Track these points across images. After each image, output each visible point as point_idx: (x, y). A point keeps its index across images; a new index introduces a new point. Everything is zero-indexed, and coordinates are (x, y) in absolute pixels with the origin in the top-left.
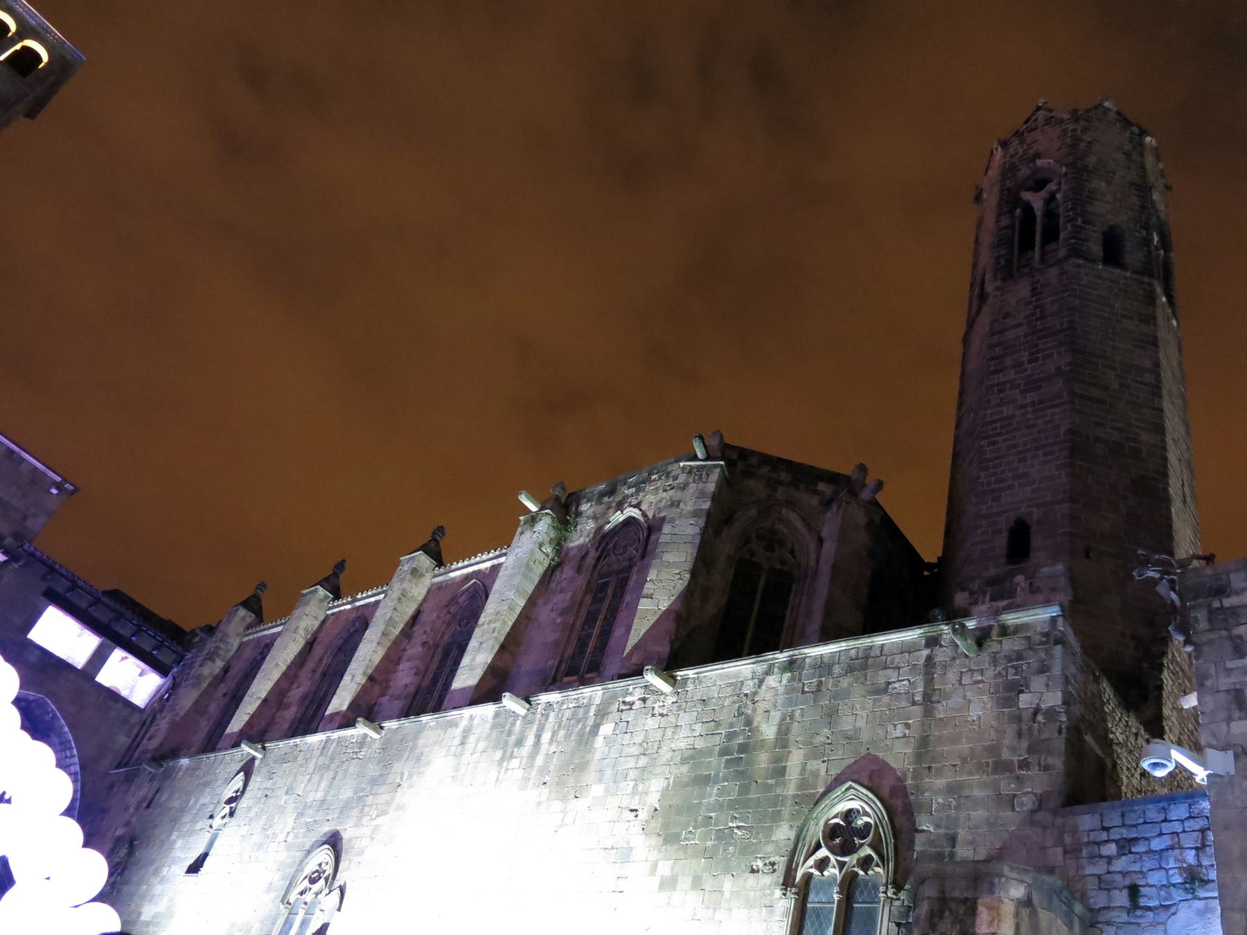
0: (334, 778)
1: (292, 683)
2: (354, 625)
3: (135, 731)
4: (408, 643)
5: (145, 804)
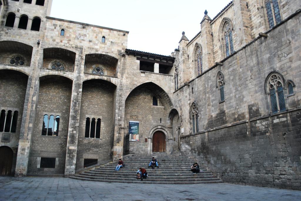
0: (257, 55)
1: (213, 46)
3: (174, 81)
4: (250, 12)
5: (191, 93)
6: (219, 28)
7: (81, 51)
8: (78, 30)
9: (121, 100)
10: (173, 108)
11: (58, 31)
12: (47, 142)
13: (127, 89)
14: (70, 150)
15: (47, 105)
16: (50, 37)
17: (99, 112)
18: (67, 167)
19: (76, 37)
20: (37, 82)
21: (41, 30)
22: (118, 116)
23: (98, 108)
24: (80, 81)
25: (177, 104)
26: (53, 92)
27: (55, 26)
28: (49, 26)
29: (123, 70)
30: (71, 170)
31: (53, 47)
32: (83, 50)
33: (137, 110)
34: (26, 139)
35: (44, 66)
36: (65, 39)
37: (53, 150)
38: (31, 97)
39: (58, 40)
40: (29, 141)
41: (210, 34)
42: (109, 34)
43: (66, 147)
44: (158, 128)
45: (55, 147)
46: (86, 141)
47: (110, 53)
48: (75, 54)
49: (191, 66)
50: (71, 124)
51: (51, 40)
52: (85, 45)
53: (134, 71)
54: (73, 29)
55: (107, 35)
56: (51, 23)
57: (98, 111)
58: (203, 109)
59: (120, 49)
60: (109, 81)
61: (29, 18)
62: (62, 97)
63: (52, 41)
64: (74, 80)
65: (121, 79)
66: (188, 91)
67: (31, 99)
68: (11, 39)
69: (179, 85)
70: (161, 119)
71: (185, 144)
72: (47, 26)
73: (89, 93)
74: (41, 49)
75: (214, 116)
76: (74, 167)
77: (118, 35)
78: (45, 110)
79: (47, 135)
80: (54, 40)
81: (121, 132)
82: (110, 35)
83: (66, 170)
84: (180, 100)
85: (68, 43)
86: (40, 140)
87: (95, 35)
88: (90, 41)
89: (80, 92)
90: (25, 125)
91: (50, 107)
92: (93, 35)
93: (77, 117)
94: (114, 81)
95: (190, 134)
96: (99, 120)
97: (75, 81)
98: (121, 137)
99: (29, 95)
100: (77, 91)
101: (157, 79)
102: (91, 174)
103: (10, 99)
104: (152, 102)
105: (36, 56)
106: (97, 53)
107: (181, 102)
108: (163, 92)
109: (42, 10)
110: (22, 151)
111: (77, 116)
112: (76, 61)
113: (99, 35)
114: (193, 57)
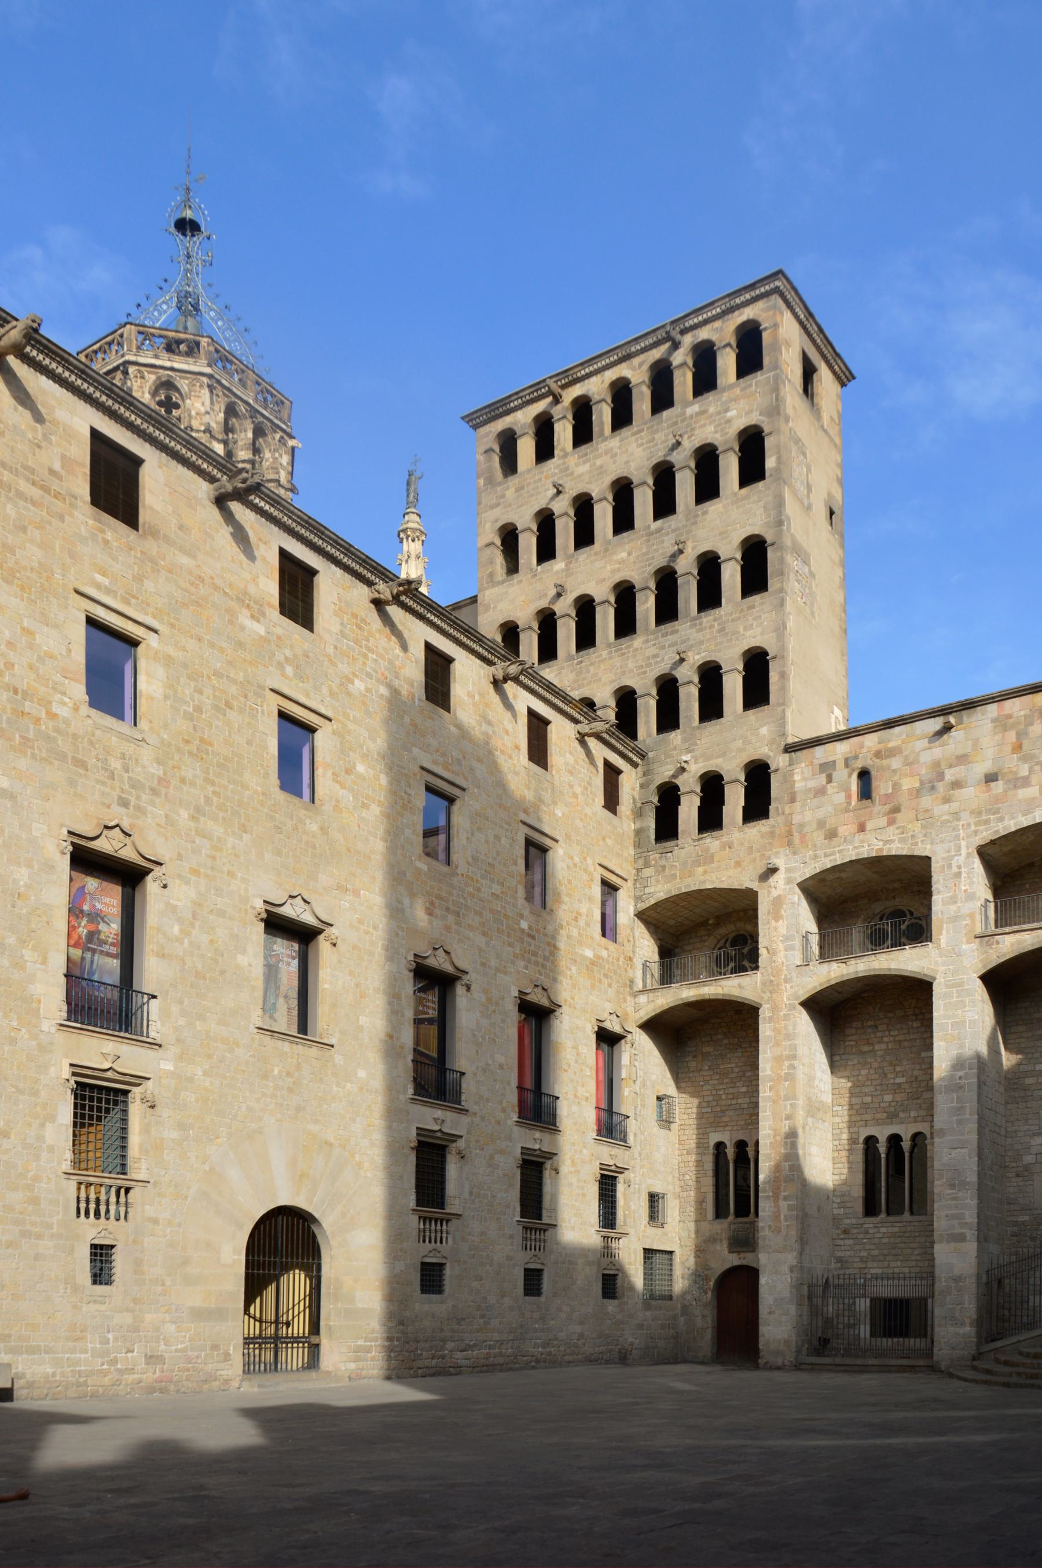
19: (922, 783)
27: (827, 768)
28: (804, 779)
54: (905, 753)
56: (812, 763)
72: (797, 785)
109: (765, 725)
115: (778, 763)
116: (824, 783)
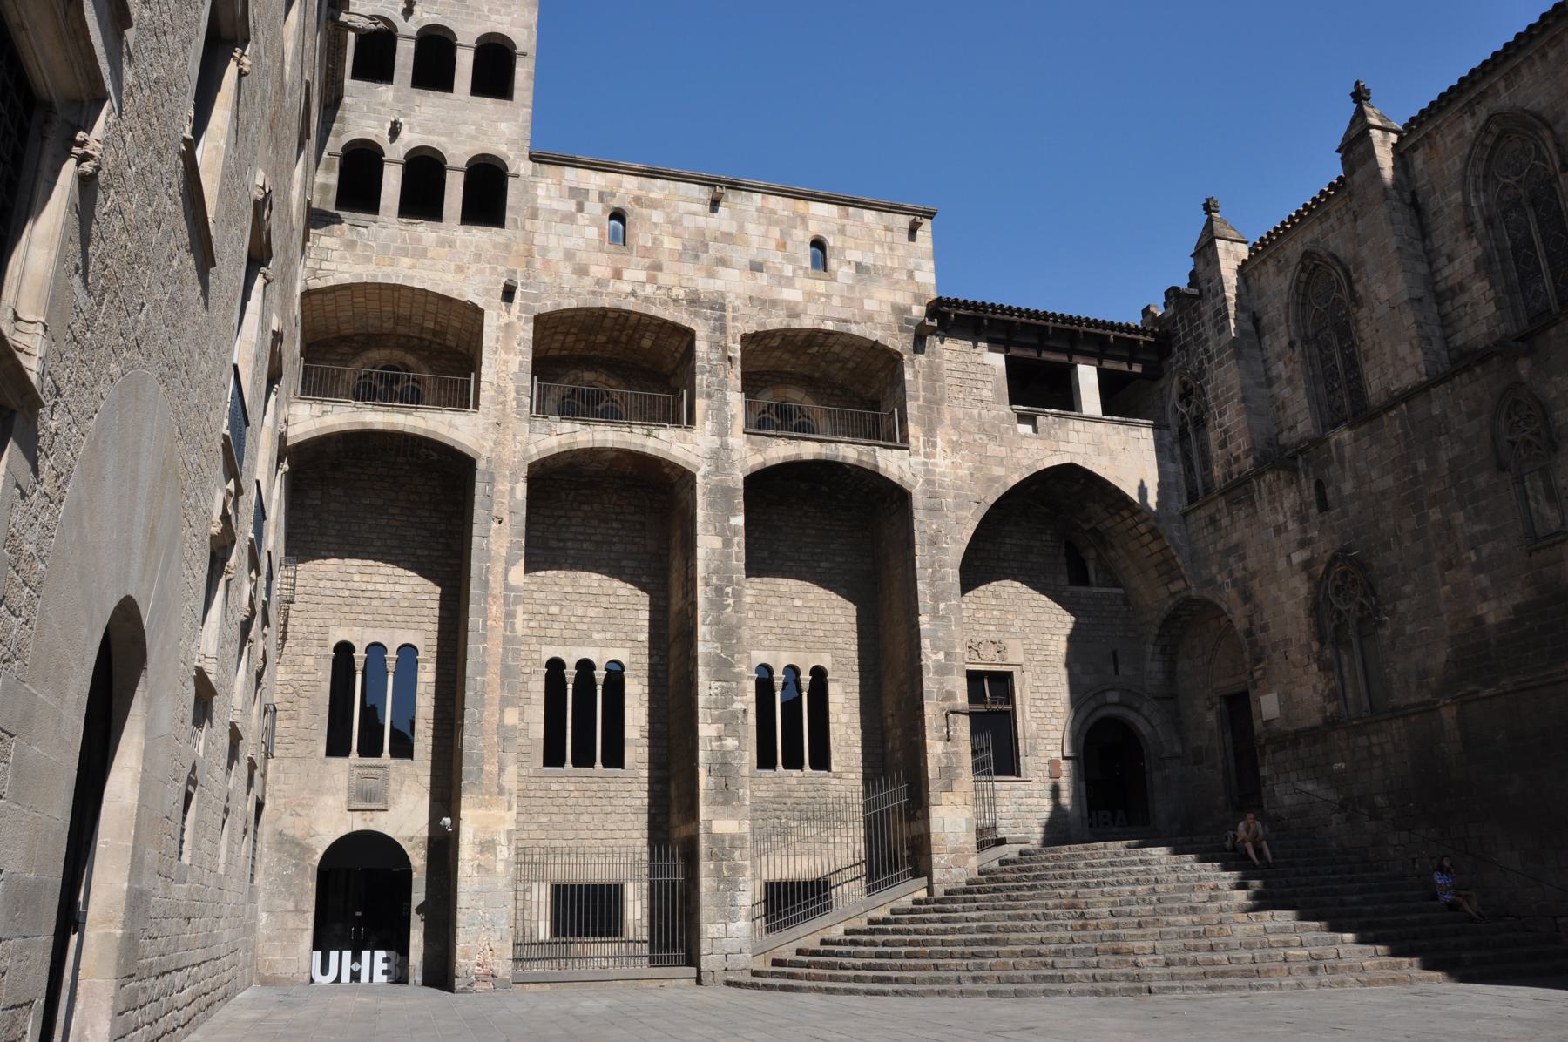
2: (1488, 132)
3: (1178, 450)
5: (1314, 510)
6: (1459, 166)
7: (715, 319)
8: (695, 214)
9: (939, 566)
10: (1185, 594)
11: (594, 221)
12: (571, 802)
13: (960, 507)
14: (716, 839)
15: (554, 610)
16: (560, 255)
17: (816, 633)
18: (711, 929)
20: (521, 490)
21: (516, 221)
22: (936, 649)
23: (808, 611)
24: (729, 475)
25: (1215, 569)
26: (582, 537)
27: (579, 195)
28: (549, 197)
29: (931, 409)
30: (731, 945)
31: (581, 305)
32: (729, 315)
33: (995, 613)
34: (496, 789)
35: (541, 408)
36: (635, 259)
37: (606, 842)
38: (499, 567)
39: (600, 270)
40: (509, 802)
41: (1402, 200)
42: (844, 226)
43: (699, 823)
44: (1106, 704)
45: (612, 826)
46: (764, 788)
47: (856, 322)
48: (688, 335)
49: (1279, 368)
50: (707, 701)
51: (569, 270)
52: (732, 284)
53: (984, 412)
55: (832, 233)
57: (808, 626)
58: (1408, 589)
59: (902, 298)
60: (869, 468)
61: (449, 163)
62: (623, 564)
63: (573, 273)
64: (698, 469)
65: (927, 455)
66: (1290, 499)
67: (500, 578)
68: (375, 276)
69: (1217, 471)
70: (1114, 653)
71: (1293, 777)
72: (539, 201)
73: (757, 535)
74: (524, 316)
75: (1491, 619)
76: (741, 926)
77: (887, 229)
78: (550, 633)
79: (569, 765)
80: (582, 271)
81: (955, 731)
82: (851, 228)
83: (705, 947)
84: (1237, 550)
85: (652, 280)
86: (539, 794)
87: (775, 232)
88: (756, 267)
89: (736, 534)
90: (481, 713)
91: (572, 619)
92: (766, 236)
93: (733, 666)
94: (895, 466)
95: (1325, 720)
96: (819, 674)
97: (704, 477)
98: (958, 761)
99: (489, 558)
100: (723, 528)
101: (1099, 447)
102: (859, 962)
103: (370, 587)
104: (1065, 569)
105: (503, 355)
106: (795, 324)
107: (1243, 558)
108: (1126, 514)
109: (507, 120)
110: (481, 852)
111: (733, 657)
112: (702, 373)
113: (794, 231)
114: (1293, 327)
115: (519, 169)
116: (574, 208)
